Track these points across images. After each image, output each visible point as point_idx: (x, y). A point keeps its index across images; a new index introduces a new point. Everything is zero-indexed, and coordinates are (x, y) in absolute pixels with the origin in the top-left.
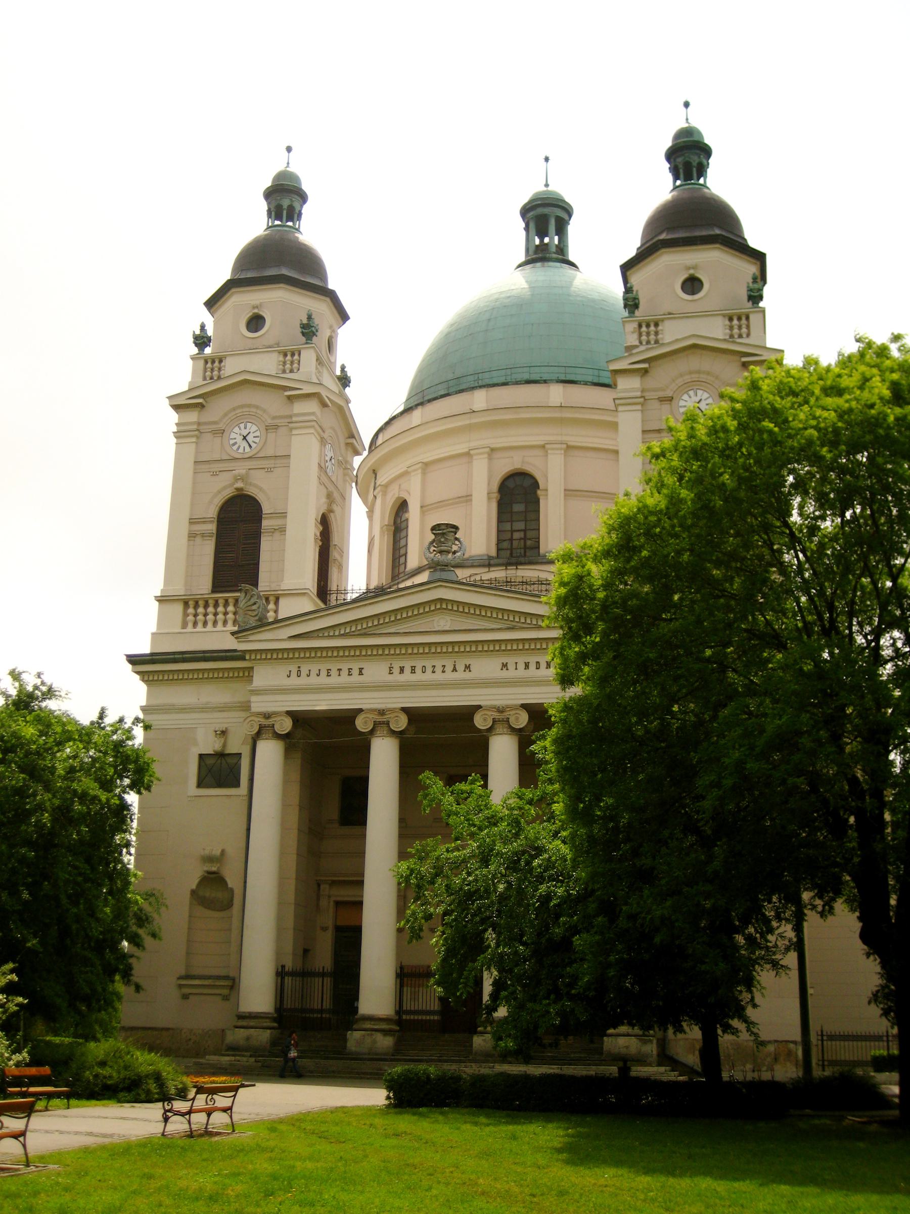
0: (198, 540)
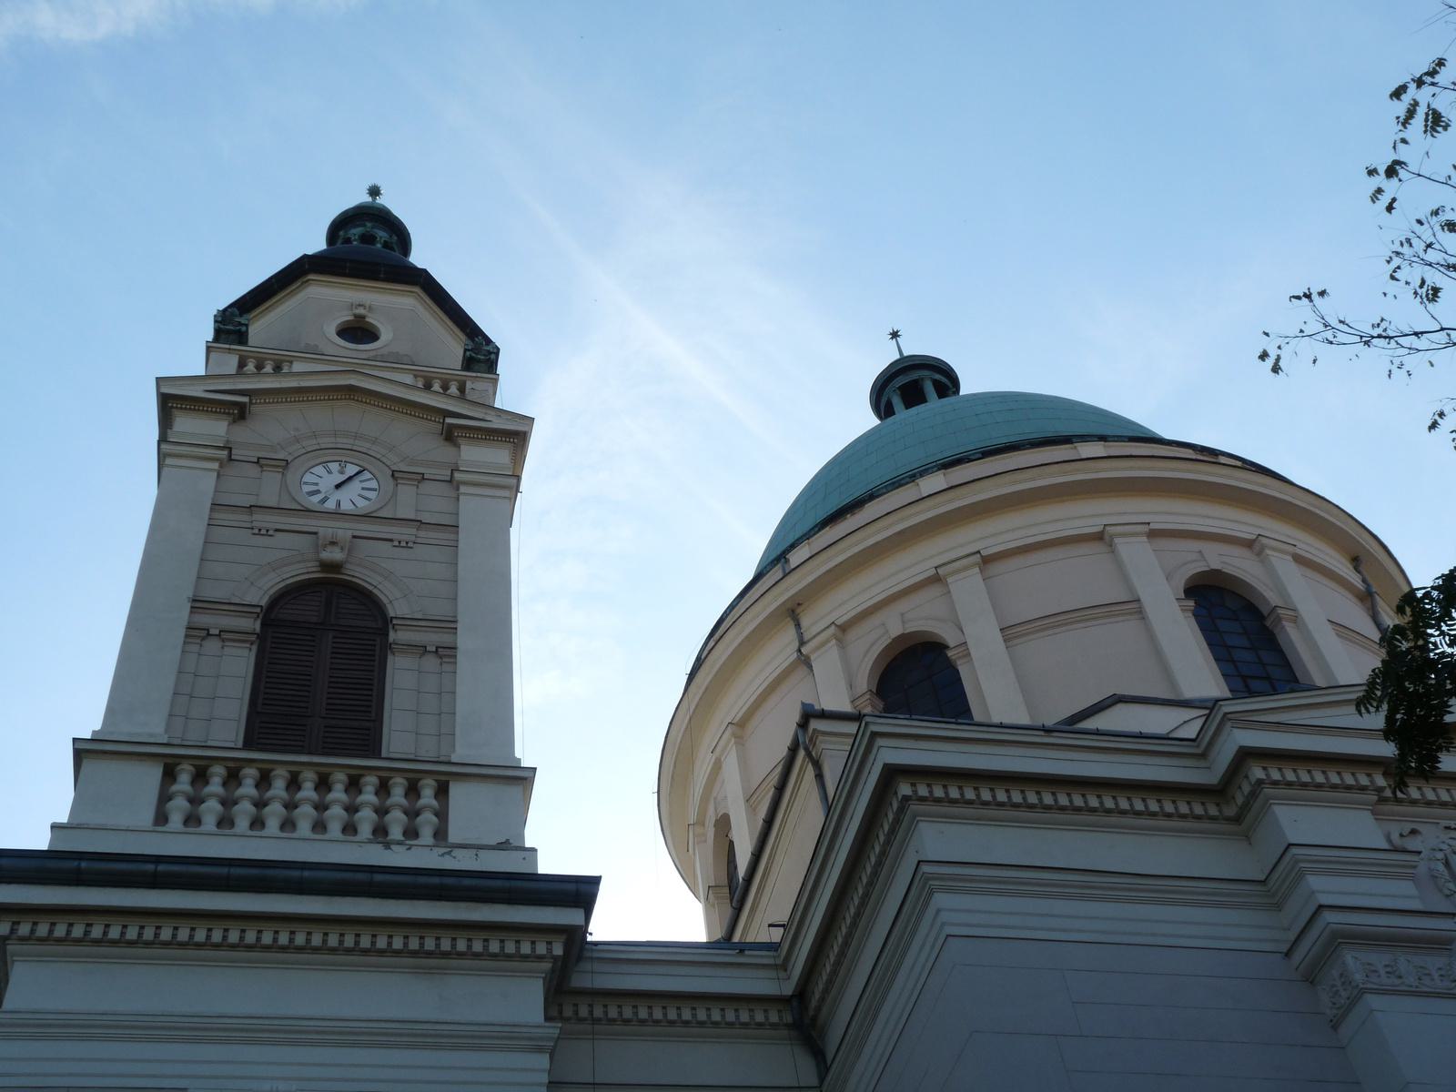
0: (212, 645)
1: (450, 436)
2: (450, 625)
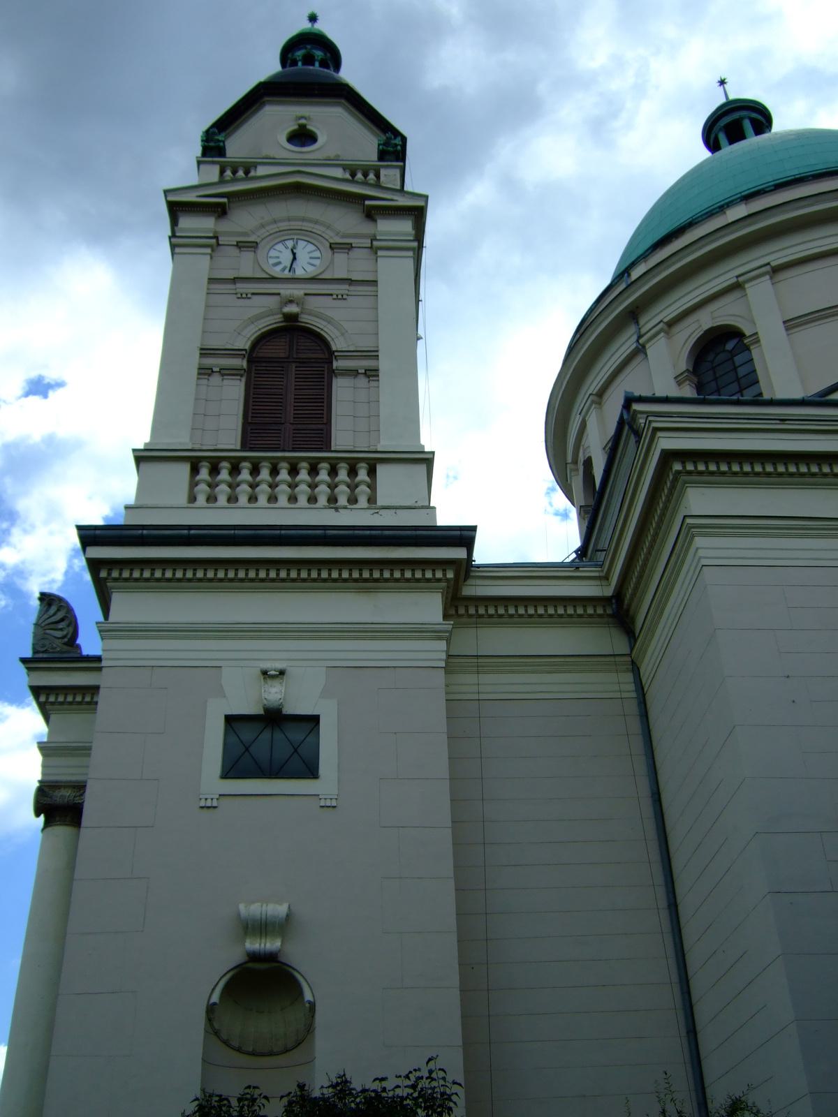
0: (216, 379)
1: (371, 214)
2: (373, 354)
